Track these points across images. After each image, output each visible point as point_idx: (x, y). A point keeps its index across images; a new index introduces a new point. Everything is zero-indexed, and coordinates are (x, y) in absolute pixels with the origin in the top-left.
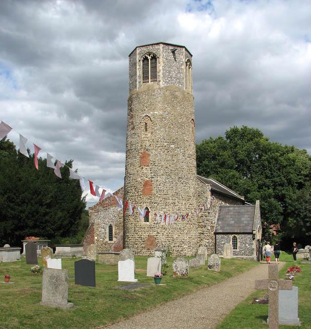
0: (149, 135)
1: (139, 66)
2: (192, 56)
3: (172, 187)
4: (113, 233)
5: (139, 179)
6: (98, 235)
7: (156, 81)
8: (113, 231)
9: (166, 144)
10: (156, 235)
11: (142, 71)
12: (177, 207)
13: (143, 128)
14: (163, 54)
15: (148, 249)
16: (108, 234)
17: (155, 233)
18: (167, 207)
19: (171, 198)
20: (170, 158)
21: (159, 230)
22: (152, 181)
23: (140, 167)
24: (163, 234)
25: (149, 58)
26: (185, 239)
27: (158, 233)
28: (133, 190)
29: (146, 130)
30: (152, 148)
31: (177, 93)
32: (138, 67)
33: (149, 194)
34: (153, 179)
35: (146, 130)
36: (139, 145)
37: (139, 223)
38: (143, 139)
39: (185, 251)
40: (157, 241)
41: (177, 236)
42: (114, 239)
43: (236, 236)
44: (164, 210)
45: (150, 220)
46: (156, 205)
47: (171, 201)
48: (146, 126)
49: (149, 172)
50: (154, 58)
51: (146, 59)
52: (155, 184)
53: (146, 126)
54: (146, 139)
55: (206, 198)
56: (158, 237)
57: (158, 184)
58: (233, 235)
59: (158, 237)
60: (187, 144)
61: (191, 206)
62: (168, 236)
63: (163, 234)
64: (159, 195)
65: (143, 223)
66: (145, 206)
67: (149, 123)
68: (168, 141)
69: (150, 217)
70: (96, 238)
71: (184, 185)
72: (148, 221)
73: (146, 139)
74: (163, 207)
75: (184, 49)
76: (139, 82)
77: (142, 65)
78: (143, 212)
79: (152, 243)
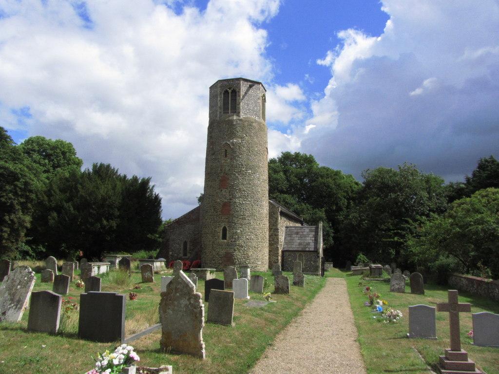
1: (221, 97)
2: (266, 91)
4: (188, 249)
5: (219, 200)
6: (172, 251)
7: (236, 112)
8: (188, 247)
11: (222, 103)
13: (223, 154)
14: (243, 88)
17: (232, 251)
22: (230, 203)
23: (219, 189)
25: (230, 91)
29: (226, 156)
31: (254, 124)
32: (219, 99)
35: (226, 156)
36: (219, 169)
39: (259, 268)
41: (252, 253)
42: (189, 255)
43: (302, 253)
45: (227, 238)
48: (226, 153)
50: (235, 93)
51: (226, 92)
53: (226, 153)
54: (226, 164)
55: (276, 218)
58: (299, 253)
66: (223, 225)
67: (229, 151)
69: (228, 235)
70: (171, 253)
73: (226, 164)
75: (261, 85)
76: (220, 113)
77: (223, 97)
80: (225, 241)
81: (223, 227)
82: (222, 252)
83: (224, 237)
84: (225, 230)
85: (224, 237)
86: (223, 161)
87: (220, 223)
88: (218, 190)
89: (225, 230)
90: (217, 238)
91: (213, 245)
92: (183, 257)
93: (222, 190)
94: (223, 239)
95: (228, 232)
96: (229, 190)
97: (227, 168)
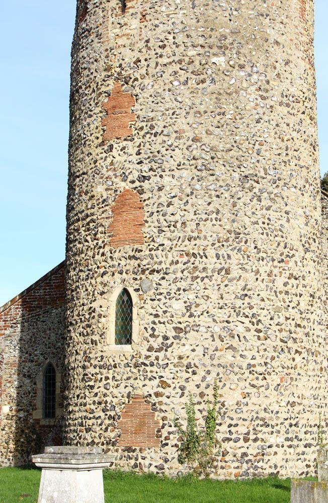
0: (135, 23)
3: (218, 212)
9: (192, 52)
10: (157, 395)
12: (236, 287)
15: (129, 449)
16: (40, 394)
17: (152, 387)
18: (199, 285)
19: (211, 252)
20: (209, 103)
21: (167, 375)
22: (141, 192)
24: (182, 388)
26: (275, 407)
27: (164, 384)
28: (82, 230)
30: (143, 71)
33: (134, 241)
34: (146, 185)
37: (99, 346)
38: (112, 44)
40: (158, 416)
44: (184, 296)
45: (135, 337)
46: (156, 277)
47: (211, 263)
49: (135, 158)
52: (152, 200)
56: (164, 399)
57: (164, 200)
59: (164, 399)
60: (278, 54)
61: (293, 281)
62: (202, 395)
63: (182, 388)
64: (167, 243)
65: (111, 348)
68: (201, 41)
71: (266, 202)
72: (129, 341)
74: (183, 285)
78: (109, 306)
79: (142, 424)
80: (127, 348)
81: (117, 291)
82: (117, 394)
83: (125, 335)
84: (125, 304)
85: (125, 335)
86: (112, 32)
87: (106, 278)
88: (99, 150)
89: (125, 304)
90: (96, 338)
91: (84, 367)
92: (43, 423)
93: (111, 147)
94: (119, 342)
95: (135, 310)
96: (137, 141)
97: (129, 57)
